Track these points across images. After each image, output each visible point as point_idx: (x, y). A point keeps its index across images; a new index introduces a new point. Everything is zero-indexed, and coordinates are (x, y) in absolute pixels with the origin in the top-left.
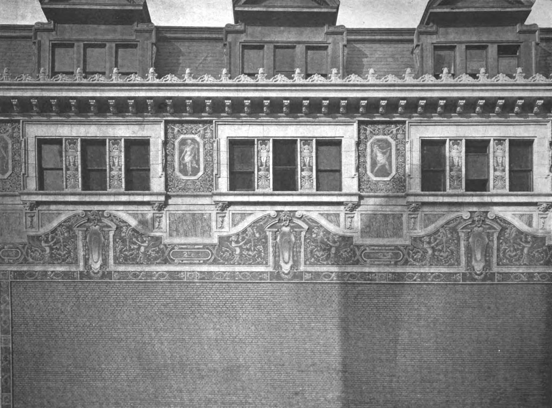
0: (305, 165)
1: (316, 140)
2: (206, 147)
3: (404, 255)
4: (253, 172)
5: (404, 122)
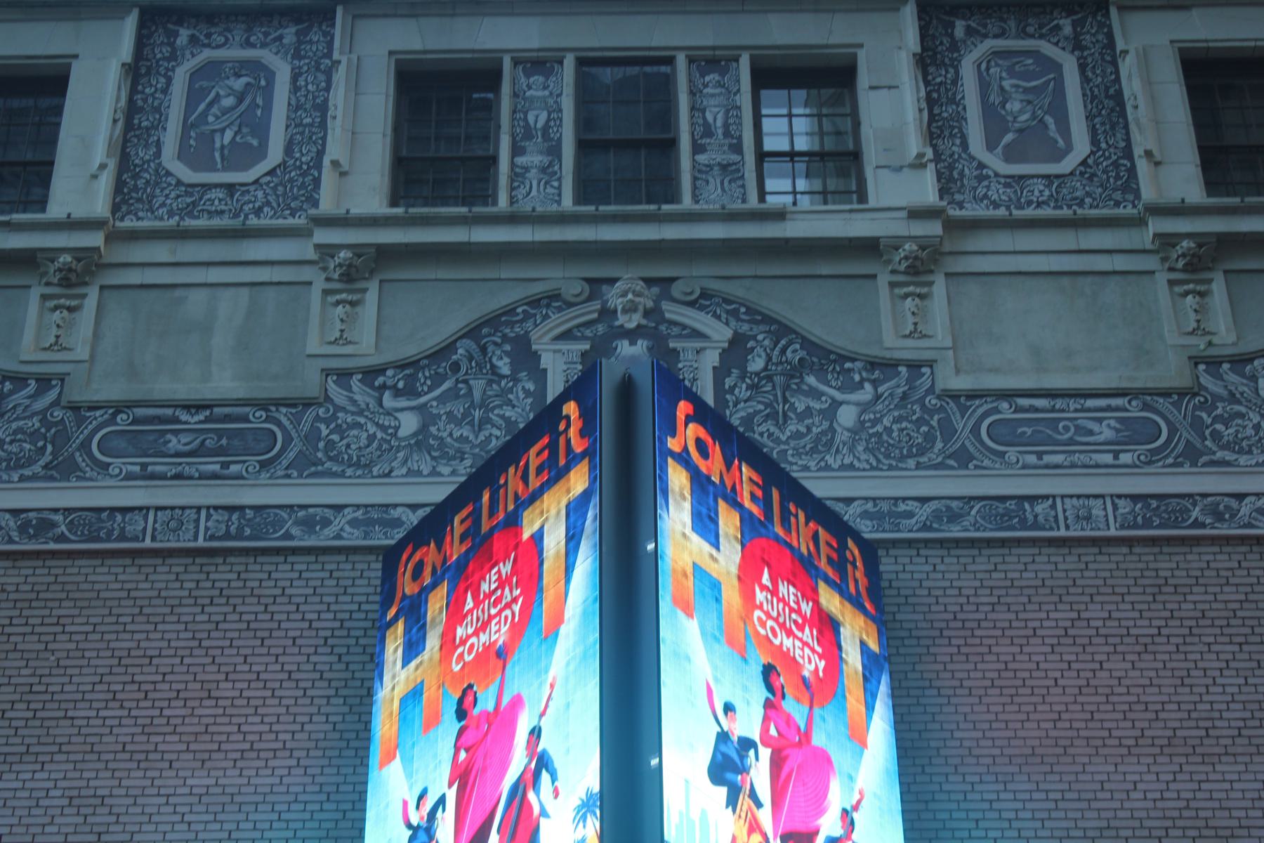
0: (708, 132)
1: (753, 60)
2: (301, 82)
3: (1173, 430)
4: (494, 160)
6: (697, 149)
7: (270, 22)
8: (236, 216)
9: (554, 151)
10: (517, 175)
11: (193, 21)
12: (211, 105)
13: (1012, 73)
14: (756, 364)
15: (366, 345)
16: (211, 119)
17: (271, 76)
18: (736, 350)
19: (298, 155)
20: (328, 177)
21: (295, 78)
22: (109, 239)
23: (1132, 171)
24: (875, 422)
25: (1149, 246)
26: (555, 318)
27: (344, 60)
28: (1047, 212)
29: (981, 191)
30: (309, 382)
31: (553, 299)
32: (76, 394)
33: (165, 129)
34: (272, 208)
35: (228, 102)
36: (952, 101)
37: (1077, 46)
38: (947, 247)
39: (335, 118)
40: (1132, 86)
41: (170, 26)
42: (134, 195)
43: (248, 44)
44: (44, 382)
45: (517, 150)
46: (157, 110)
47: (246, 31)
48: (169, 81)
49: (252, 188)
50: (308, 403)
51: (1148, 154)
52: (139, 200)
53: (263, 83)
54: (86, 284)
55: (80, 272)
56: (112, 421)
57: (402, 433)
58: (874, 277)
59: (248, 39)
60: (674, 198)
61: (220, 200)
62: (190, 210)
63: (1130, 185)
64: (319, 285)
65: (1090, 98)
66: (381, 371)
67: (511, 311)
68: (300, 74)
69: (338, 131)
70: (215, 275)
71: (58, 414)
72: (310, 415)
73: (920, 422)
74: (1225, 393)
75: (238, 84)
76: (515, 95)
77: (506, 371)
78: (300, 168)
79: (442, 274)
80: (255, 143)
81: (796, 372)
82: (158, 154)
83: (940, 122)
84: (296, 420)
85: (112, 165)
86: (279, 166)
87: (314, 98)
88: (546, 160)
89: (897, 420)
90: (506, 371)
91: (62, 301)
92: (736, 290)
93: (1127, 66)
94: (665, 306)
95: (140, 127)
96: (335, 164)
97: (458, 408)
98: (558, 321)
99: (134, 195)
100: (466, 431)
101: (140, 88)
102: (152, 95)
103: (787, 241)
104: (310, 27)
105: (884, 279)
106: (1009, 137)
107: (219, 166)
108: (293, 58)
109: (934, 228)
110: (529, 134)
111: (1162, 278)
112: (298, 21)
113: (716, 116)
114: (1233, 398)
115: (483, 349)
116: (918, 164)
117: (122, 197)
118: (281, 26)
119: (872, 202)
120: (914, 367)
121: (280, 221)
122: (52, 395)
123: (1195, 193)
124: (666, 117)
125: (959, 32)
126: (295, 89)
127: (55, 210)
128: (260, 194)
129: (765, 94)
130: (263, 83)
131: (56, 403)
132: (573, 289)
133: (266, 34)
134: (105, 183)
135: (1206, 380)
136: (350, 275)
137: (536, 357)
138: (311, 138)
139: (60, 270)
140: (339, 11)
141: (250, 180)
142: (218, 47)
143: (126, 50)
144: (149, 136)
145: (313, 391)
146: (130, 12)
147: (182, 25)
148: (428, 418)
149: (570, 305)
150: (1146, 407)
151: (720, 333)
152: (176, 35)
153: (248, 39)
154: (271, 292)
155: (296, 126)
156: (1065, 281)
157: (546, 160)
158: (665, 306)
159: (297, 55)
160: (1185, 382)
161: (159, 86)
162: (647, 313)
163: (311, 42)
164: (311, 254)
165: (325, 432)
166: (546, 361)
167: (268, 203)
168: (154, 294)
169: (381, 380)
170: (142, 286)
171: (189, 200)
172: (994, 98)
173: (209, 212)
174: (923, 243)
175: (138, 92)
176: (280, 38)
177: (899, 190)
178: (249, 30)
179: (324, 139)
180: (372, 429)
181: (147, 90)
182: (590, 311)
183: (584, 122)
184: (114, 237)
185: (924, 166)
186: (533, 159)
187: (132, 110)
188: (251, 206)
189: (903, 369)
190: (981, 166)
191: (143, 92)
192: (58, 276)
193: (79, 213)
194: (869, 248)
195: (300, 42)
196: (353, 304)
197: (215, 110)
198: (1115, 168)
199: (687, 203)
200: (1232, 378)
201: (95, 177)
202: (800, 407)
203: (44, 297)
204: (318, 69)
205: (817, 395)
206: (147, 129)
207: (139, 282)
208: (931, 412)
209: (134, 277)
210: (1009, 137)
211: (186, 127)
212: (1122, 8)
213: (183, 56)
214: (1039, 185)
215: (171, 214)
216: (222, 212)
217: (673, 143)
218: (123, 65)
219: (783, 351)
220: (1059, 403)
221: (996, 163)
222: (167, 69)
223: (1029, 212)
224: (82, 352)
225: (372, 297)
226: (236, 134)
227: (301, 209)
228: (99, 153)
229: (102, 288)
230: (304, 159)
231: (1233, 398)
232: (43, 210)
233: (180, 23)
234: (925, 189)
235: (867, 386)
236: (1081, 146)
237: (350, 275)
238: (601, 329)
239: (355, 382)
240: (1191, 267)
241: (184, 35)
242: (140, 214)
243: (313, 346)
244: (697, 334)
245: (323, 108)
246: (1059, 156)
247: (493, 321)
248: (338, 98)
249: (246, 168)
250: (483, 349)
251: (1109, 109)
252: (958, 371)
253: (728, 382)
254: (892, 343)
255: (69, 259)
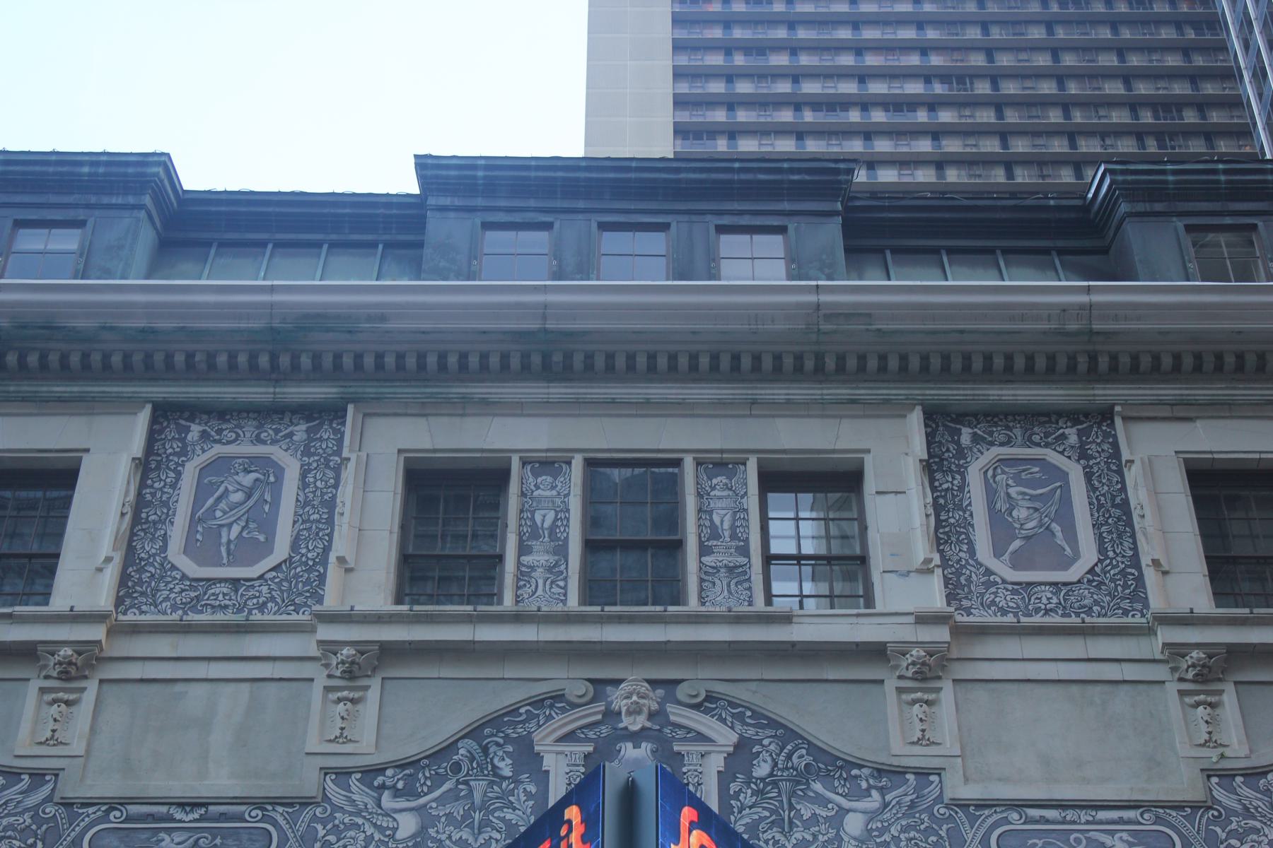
0: (715, 535)
4: (500, 558)
5: (1106, 415)
6: (704, 550)
7: (282, 419)
8: (240, 611)
9: (561, 550)
10: (523, 574)
11: (205, 417)
12: (219, 499)
13: (1019, 482)
14: (762, 770)
15: (366, 745)
16: (218, 514)
17: (280, 472)
18: (741, 754)
19: (304, 551)
20: (333, 573)
21: (303, 476)
22: (109, 633)
23: (1140, 579)
24: (882, 831)
25: (1158, 656)
26: (559, 719)
27: (353, 457)
28: (1055, 619)
29: (988, 597)
30: (307, 782)
31: (556, 699)
32: (71, 789)
33: (172, 523)
34: (277, 604)
35: (237, 497)
36: (959, 507)
37: (1083, 455)
38: (954, 654)
39: (342, 514)
40: (1138, 495)
41: (183, 422)
42: (138, 588)
43: (259, 440)
44: (38, 777)
45: (523, 550)
46: (165, 504)
47: (257, 428)
48: (179, 475)
49: (257, 583)
50: (305, 803)
51: (1156, 563)
52: (143, 594)
53: (272, 479)
54: (86, 677)
55: (79, 666)
56: (105, 818)
57: (400, 835)
58: (882, 682)
59: (258, 436)
60: (679, 599)
61: (224, 595)
62: (193, 605)
63: (1138, 594)
64: (321, 681)
65: (1096, 506)
66: (381, 770)
67: (514, 711)
68: (309, 471)
69: (345, 527)
70: (216, 670)
71: (51, 810)
72: (307, 814)
73: (928, 831)
74: (1238, 807)
75: (248, 480)
76: (523, 494)
77: (507, 772)
78: (306, 564)
79: (446, 672)
80: (262, 538)
81: (802, 778)
82: (164, 548)
83: (947, 527)
84: (293, 822)
85: (118, 558)
86: (285, 561)
87: (323, 494)
88: (552, 559)
89: (904, 830)
90: (507, 772)
91: (61, 695)
92: (740, 693)
93: (1133, 476)
94: (670, 708)
95: (147, 522)
96: (341, 560)
97: (458, 810)
98: (562, 722)
99: (138, 588)
100: (465, 834)
101: (149, 482)
102: (161, 489)
103: (793, 644)
104: (321, 425)
105: (891, 684)
106: (1017, 544)
107: (225, 561)
108: (302, 455)
109: (941, 634)
110: (535, 533)
111: (1173, 688)
112: (309, 419)
113: (723, 519)
114: (1247, 813)
115: (485, 750)
116: (925, 570)
117: (126, 590)
118: (292, 423)
119: (879, 607)
120: (923, 774)
121: (284, 617)
122: (45, 791)
123: (1203, 602)
124: (673, 519)
125: (966, 438)
126: (304, 485)
127: (59, 602)
128: (265, 589)
129: (772, 497)
130: (272, 479)
131: (48, 799)
132: (577, 690)
133: (277, 431)
134: (110, 576)
135: (1219, 794)
136: (352, 673)
137: (538, 758)
138: (317, 534)
139: (60, 663)
140: (350, 409)
141: (255, 575)
142: (229, 443)
143: (137, 446)
144: (156, 529)
145: (311, 790)
146: (143, 407)
147: (193, 422)
148: (427, 820)
149: (574, 706)
150: (1158, 820)
151: (726, 737)
152: (188, 430)
153: (258, 436)
154: (272, 688)
155: (304, 522)
156: (1075, 689)
157: (552, 559)
158: (670, 708)
159: (307, 452)
160: (1198, 795)
161: (168, 480)
162: (651, 716)
163: (321, 439)
164: (314, 651)
165: (321, 833)
166: (549, 762)
167: (273, 599)
168: (155, 687)
169: (380, 779)
170: (142, 681)
171: (193, 594)
172: (1001, 505)
173: (213, 607)
174: (932, 650)
175: (147, 487)
176: (291, 435)
177: (907, 594)
178: (260, 426)
179: (331, 535)
180: (370, 830)
181: (156, 485)
182: (594, 712)
183: (592, 521)
184: (117, 630)
185: (931, 571)
186: (540, 557)
187: (140, 503)
188: (255, 601)
189: (911, 777)
190: (989, 572)
191: (152, 487)
192: (58, 668)
193: (81, 606)
194: (876, 652)
195: (310, 439)
196: (353, 701)
197: (223, 505)
198: (1122, 576)
199: (693, 604)
200: (1246, 791)
201: (100, 570)
202: (806, 814)
203: (43, 690)
204: (327, 466)
205: (824, 802)
206: (155, 523)
207: (139, 677)
208: (940, 821)
209: (134, 671)
210: (1017, 544)
211: (194, 521)
212: (1124, 419)
213: (194, 451)
214: (1046, 593)
215: (174, 608)
216: (226, 607)
217: (679, 545)
218: (134, 459)
219: (789, 757)
220: (1070, 815)
221: (1003, 569)
222: (177, 463)
223: (1037, 619)
224: (78, 748)
225: (373, 695)
226: (243, 528)
227: (305, 604)
228: (106, 548)
229: (101, 681)
230: (310, 555)
231: (1247, 813)
232: (47, 604)
233: (192, 419)
234: (932, 595)
235: (874, 793)
236: (1089, 555)
237: (352, 673)
238: (605, 730)
239: (354, 780)
240: (1201, 678)
241: (195, 430)
242: (144, 608)
243: (313, 745)
244: (702, 738)
245: (331, 504)
246: (1066, 564)
247: (496, 721)
248: (346, 494)
249: (251, 563)
250: (485, 750)
251: (1116, 517)
252: (967, 780)
253: (734, 787)
254: (899, 750)
255: (70, 652)
